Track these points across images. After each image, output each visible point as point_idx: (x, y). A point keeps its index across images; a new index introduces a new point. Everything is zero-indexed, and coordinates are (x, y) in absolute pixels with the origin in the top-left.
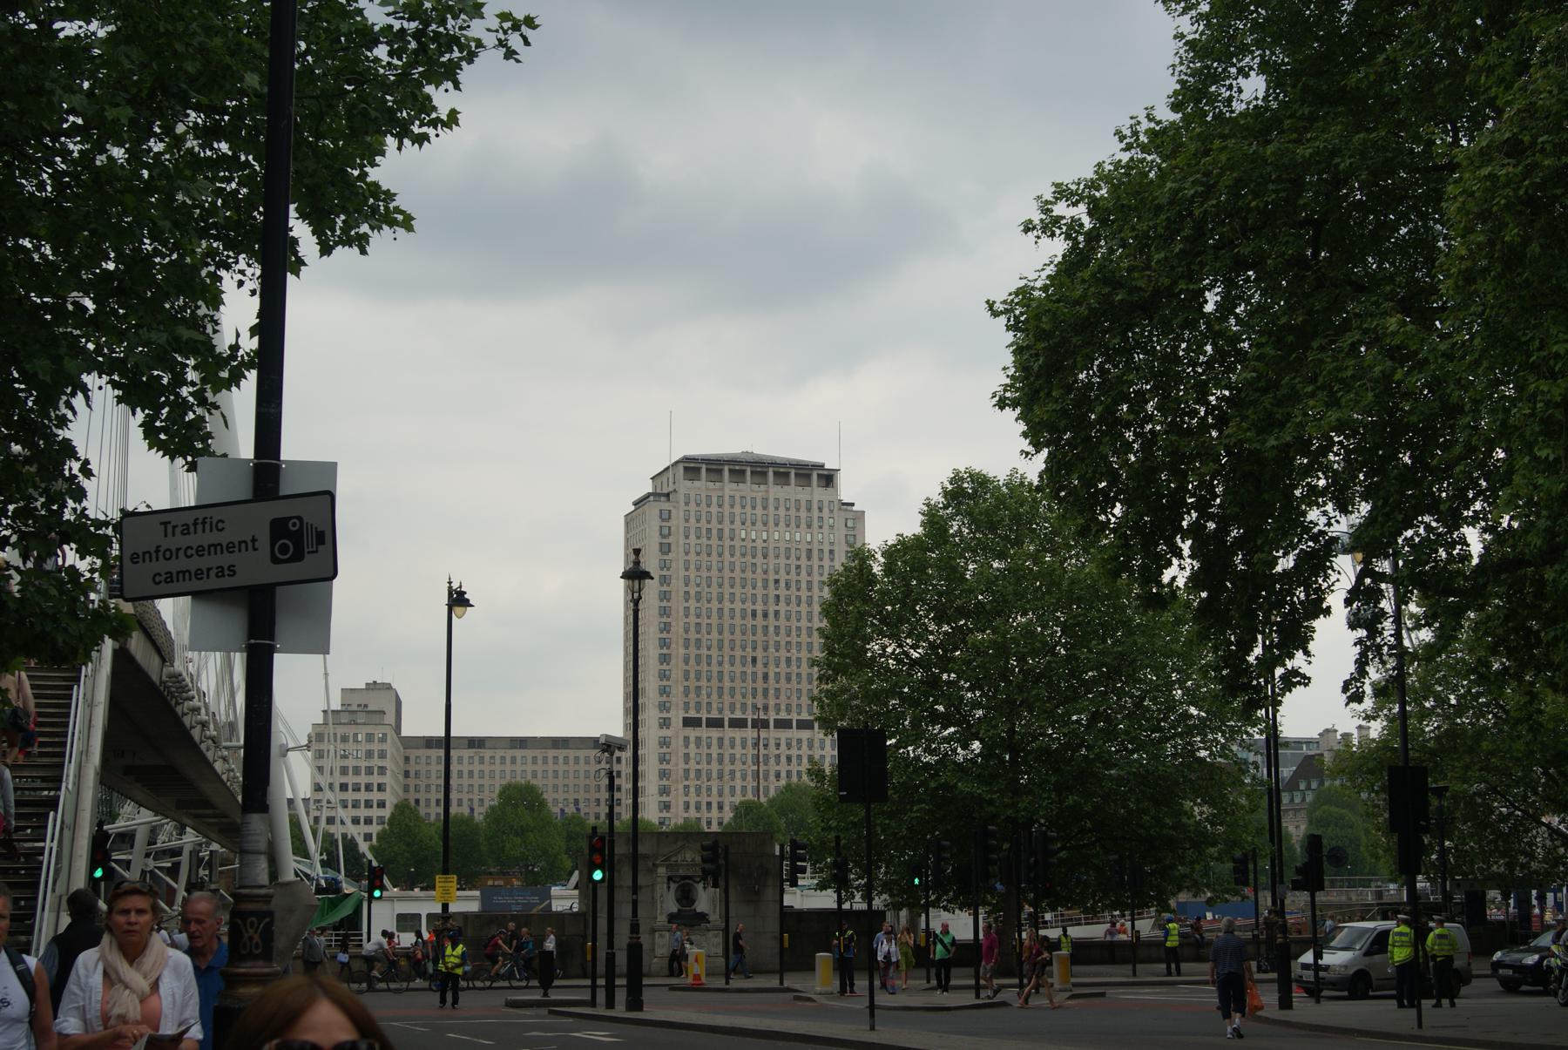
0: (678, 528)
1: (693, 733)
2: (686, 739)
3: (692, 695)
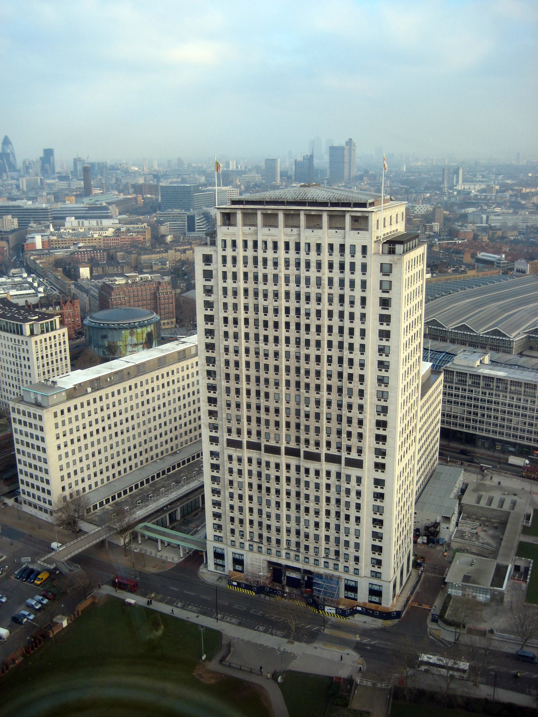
0: (217, 270)
1: (235, 453)
2: (230, 458)
3: (234, 422)
